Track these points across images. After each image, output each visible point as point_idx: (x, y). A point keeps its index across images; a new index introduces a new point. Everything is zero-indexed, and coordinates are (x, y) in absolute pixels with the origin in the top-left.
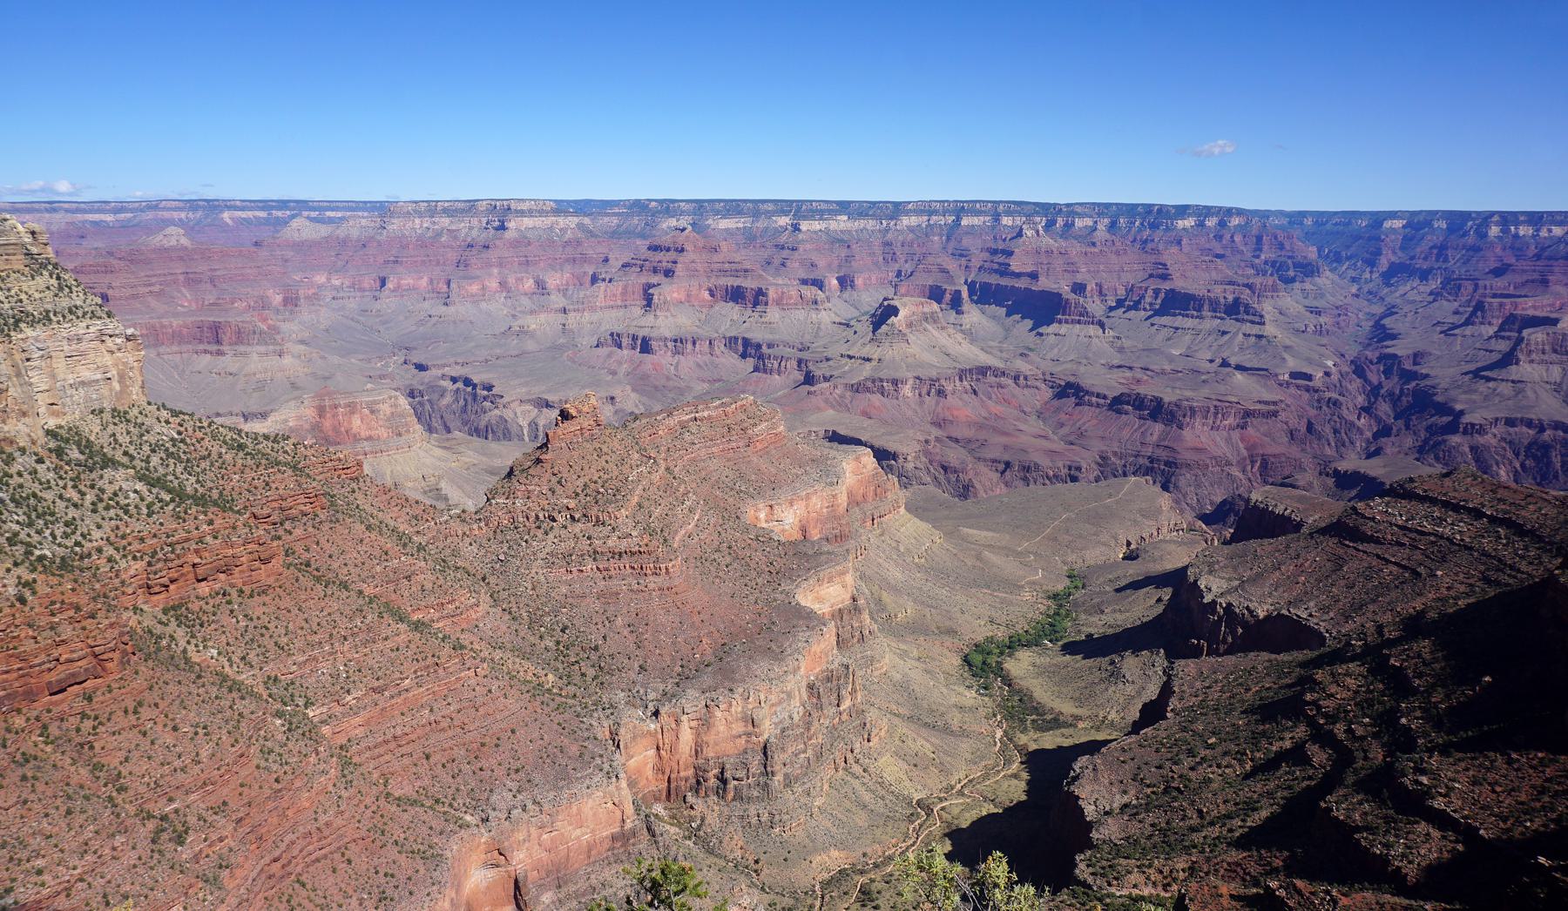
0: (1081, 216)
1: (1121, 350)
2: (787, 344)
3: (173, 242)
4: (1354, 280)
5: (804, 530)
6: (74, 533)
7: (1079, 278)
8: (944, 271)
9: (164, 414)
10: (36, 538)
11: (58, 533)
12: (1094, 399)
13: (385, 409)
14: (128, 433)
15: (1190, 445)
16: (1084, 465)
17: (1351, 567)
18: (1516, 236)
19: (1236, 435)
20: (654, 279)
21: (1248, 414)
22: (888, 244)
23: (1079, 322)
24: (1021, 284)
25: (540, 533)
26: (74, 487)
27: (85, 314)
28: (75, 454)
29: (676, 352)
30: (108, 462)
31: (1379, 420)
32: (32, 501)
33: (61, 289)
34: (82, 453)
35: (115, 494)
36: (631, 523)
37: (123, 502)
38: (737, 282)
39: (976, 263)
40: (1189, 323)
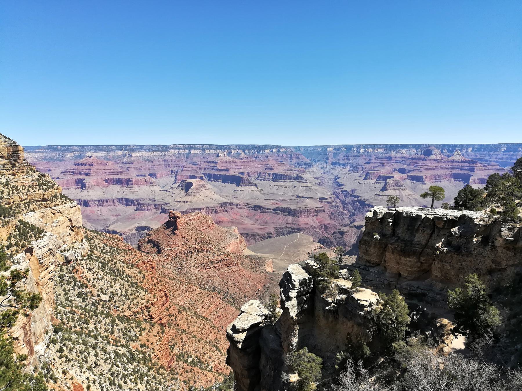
2: (144, 199)
20: (81, 177)
22: (166, 161)
23: (248, 185)
24: (223, 173)
29: (99, 205)
38: (118, 177)
39: (203, 166)
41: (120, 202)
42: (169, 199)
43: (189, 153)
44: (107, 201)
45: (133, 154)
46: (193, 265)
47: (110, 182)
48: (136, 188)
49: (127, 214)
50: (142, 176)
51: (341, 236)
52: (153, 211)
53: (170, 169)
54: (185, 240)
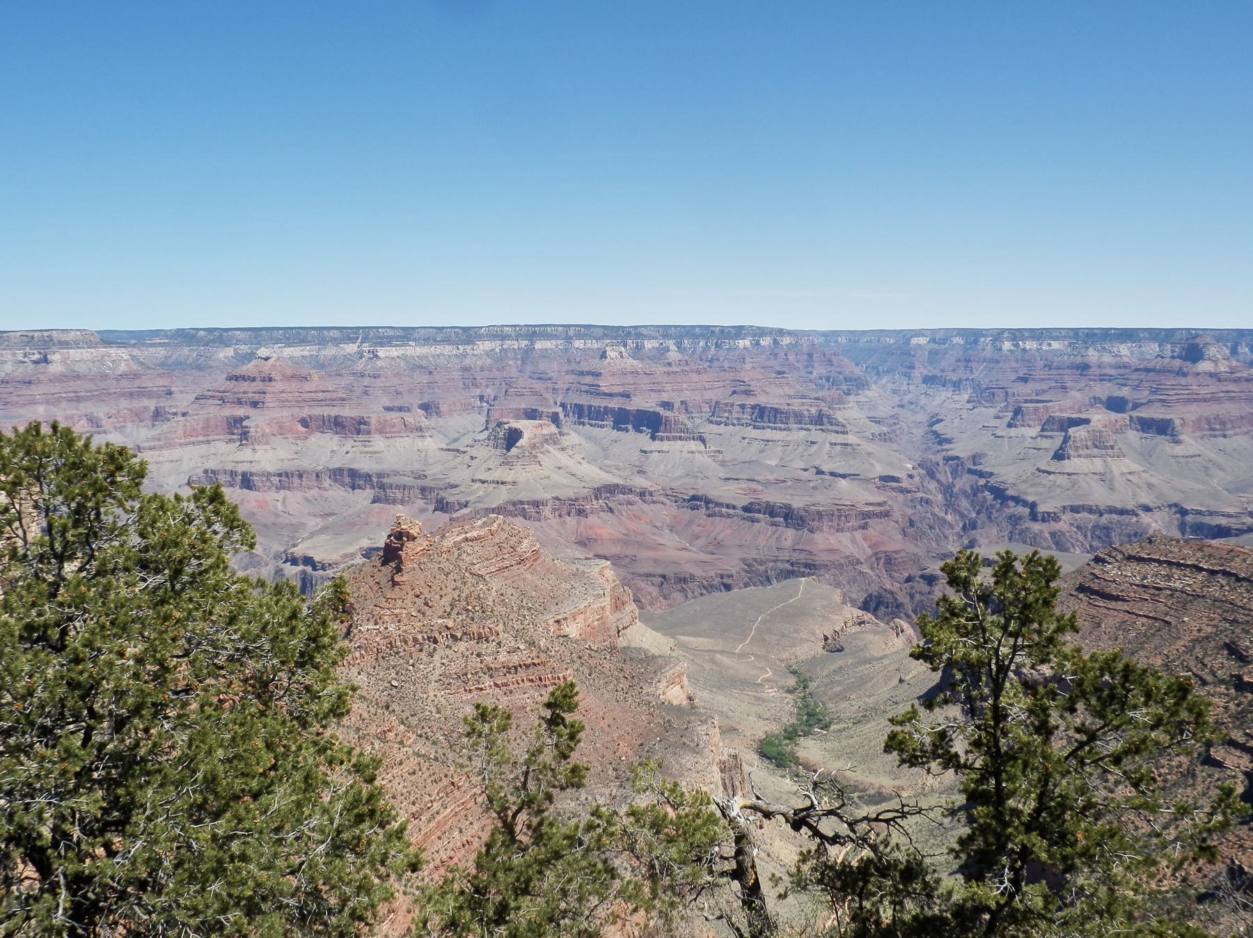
0: (650, 338)
1: (723, 464)
2: (396, 473)
4: (894, 391)
7: (665, 397)
8: (535, 393)
12: (724, 510)
15: (822, 547)
16: (734, 572)
17: (1109, 623)
18: (1024, 350)
19: (858, 535)
20: (240, 412)
21: (867, 515)
22: (467, 369)
23: (680, 439)
24: (614, 404)
25: (423, 655)
31: (962, 516)
38: (334, 412)
40: (777, 435)
41: (335, 480)
42: (461, 475)
43: (529, 350)
44: (300, 476)
45: (382, 352)
47: (313, 424)
48: (378, 443)
49: (351, 511)
50: (400, 409)
51: (927, 588)
52: (416, 505)
53: (478, 392)
54: (420, 602)
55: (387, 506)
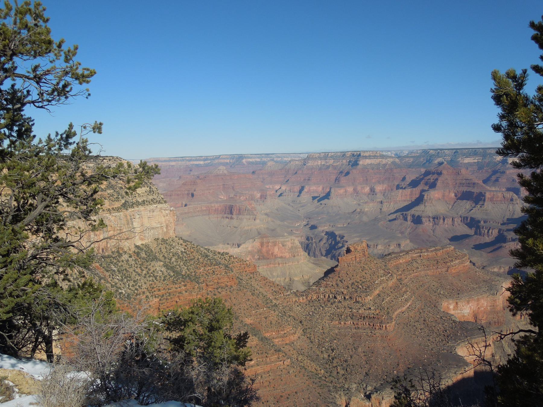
3: (221, 172)
5: (476, 317)
6: (136, 285)
9: (181, 242)
10: (123, 285)
11: (131, 284)
13: (289, 244)
14: (166, 248)
26: (140, 267)
27: (157, 201)
28: (143, 255)
30: (155, 259)
32: (125, 272)
33: (150, 192)
34: (146, 254)
35: (154, 271)
36: (372, 303)
37: (156, 274)
44: (444, 219)
46: (329, 314)
55: (480, 237)
